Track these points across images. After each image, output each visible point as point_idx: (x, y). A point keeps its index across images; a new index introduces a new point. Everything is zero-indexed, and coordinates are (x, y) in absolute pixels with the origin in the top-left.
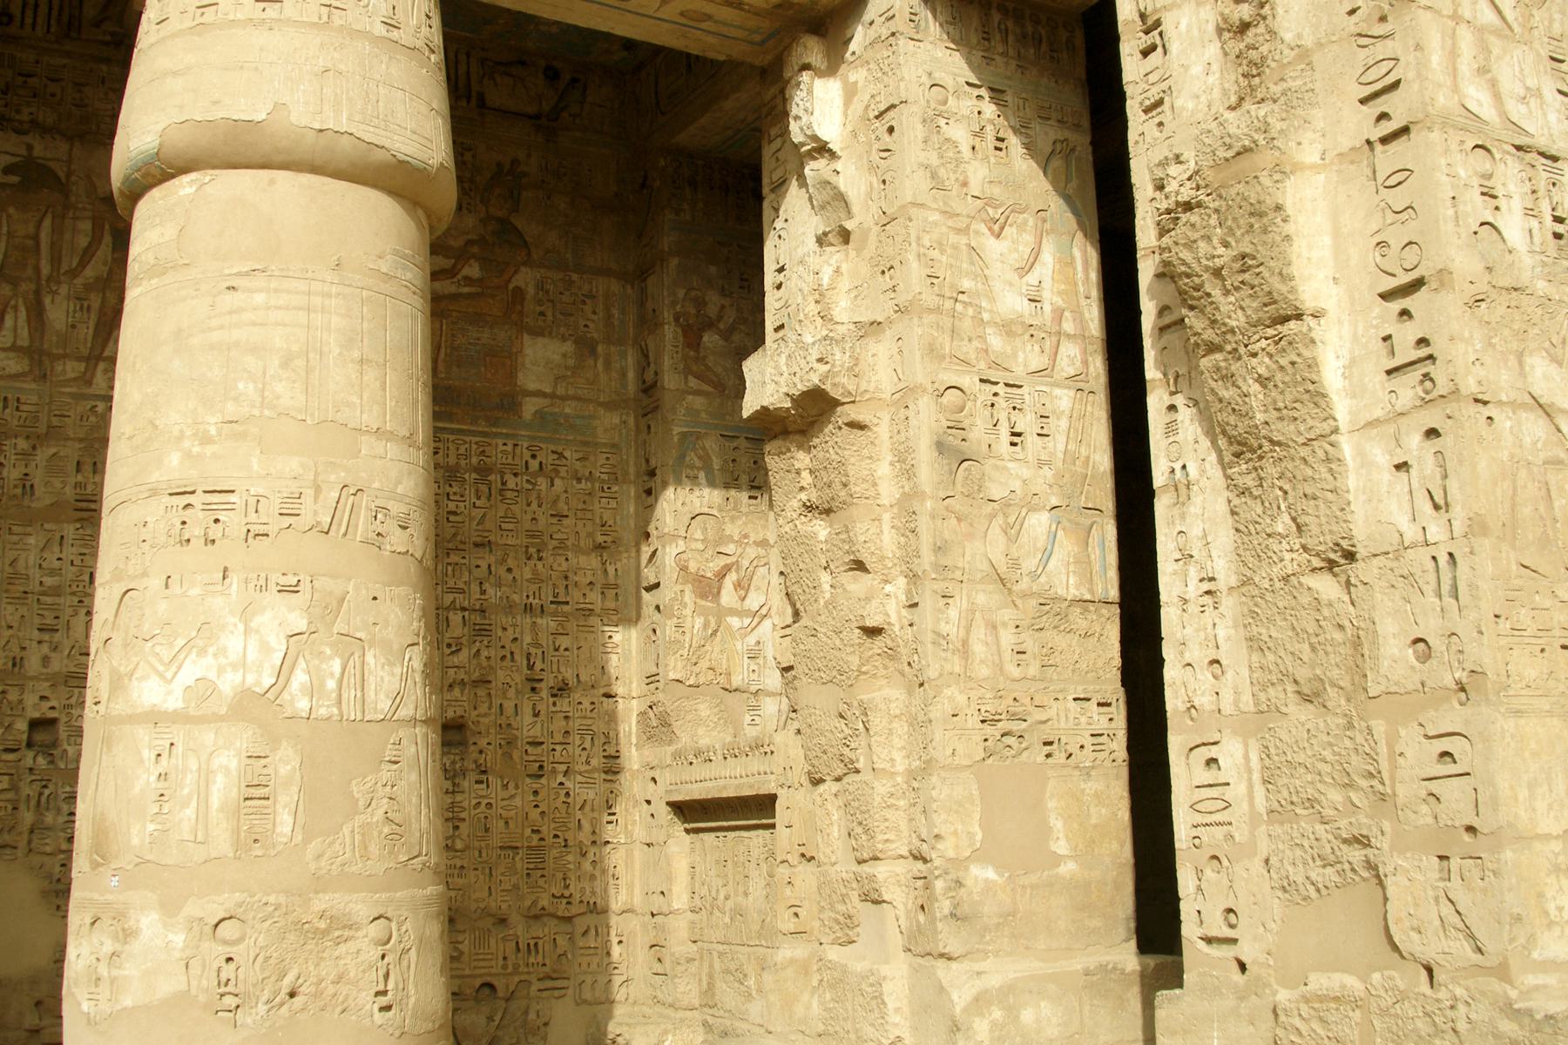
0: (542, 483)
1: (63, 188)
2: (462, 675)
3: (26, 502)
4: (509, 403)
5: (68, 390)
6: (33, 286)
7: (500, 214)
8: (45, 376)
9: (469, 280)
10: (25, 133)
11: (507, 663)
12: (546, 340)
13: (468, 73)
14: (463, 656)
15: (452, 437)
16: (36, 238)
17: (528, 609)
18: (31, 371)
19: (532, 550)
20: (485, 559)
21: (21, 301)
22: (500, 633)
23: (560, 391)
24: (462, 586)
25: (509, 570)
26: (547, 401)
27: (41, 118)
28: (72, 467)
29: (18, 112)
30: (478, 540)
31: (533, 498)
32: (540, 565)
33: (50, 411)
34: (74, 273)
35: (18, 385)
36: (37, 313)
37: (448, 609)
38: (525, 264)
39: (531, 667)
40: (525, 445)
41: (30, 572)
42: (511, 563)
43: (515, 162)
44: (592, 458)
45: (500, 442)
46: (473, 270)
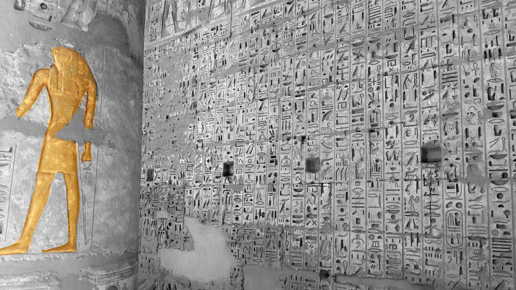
2: (434, 112)
11: (471, 98)
14: (436, 98)
17: (488, 55)
20: (449, 29)
22: (463, 77)
24: (432, 50)
28: (238, 47)
30: (444, 16)
32: (496, 20)
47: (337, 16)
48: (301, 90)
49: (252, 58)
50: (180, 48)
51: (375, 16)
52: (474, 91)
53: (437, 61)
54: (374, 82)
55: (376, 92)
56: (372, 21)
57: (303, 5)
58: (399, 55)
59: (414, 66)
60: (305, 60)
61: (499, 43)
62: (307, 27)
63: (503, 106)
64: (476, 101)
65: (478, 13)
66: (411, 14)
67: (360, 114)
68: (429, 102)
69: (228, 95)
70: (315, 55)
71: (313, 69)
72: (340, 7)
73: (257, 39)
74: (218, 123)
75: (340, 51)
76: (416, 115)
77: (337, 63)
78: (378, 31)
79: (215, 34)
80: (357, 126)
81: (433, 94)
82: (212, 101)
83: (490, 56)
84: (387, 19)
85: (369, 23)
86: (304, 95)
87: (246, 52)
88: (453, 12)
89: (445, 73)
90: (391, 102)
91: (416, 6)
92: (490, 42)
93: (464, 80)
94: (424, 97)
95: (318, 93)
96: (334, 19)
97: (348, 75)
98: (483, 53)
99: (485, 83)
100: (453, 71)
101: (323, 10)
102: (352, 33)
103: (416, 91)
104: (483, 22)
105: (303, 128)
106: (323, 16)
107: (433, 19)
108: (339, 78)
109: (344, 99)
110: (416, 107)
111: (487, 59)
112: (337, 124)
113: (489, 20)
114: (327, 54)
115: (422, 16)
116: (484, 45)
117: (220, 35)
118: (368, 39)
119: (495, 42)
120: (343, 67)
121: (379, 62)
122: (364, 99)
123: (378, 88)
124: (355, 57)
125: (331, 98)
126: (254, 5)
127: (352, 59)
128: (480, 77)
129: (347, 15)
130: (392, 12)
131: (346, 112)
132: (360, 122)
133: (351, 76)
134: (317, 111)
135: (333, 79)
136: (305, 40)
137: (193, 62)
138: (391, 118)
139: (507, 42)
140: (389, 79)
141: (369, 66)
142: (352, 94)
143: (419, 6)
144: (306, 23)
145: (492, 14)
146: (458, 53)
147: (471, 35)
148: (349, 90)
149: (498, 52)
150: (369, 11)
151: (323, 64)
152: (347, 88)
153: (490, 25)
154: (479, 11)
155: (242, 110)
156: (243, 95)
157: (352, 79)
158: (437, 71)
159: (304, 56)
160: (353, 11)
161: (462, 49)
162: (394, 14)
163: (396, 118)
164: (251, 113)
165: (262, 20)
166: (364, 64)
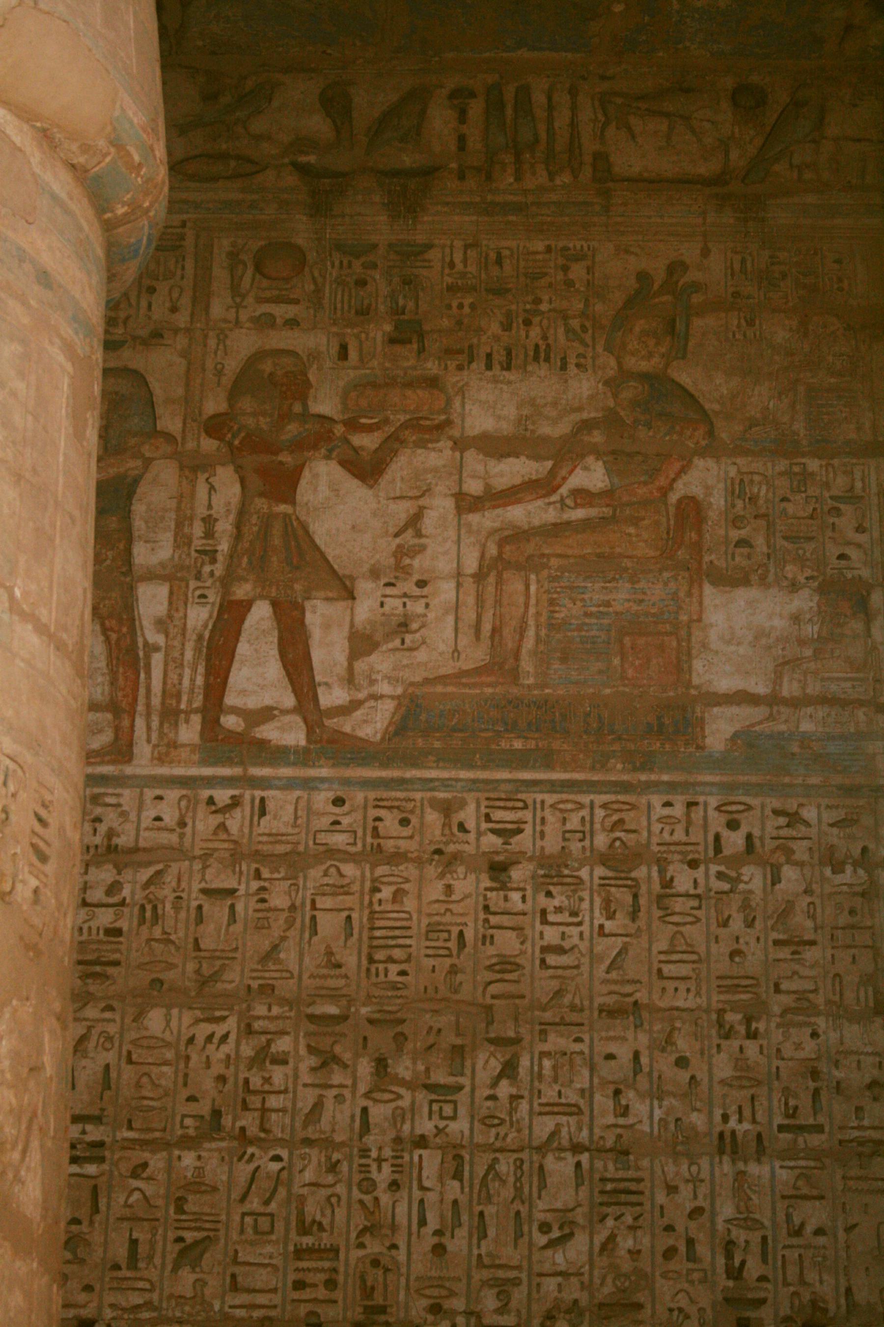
0: (753, 878)
2: (573, 1292)
4: (675, 721)
7: (644, 366)
9: (582, 496)
11: (679, 1264)
12: (754, 593)
13: (573, 125)
14: (578, 1249)
15: (550, 799)
17: (727, 1144)
19: (733, 1017)
20: (626, 1043)
22: (661, 1198)
23: (789, 688)
24: (572, 1097)
25: (682, 1062)
26: (760, 712)
30: (610, 1000)
31: (733, 909)
37: (542, 1149)
38: (703, 453)
39: (735, 1273)
40: (713, 802)
42: (683, 1044)
43: (676, 268)
44: (867, 820)
45: (656, 800)
46: (593, 476)
47: (253, 904)
48: (88, 1138)
51: (393, 942)
52: (690, 1242)
53: (585, 1133)
54: (380, 1160)
55: (385, 1199)
56: (380, 955)
57: (115, 825)
58: (467, 1089)
59: (513, 1135)
60: (112, 1029)
61: (759, 1117)
62: (126, 910)
63: (763, 1301)
64: (696, 1276)
65: (705, 1016)
66: (506, 965)
67: (327, 1264)
68: (559, 1258)
70: (155, 1020)
71: (146, 1069)
72: (266, 874)
75: (257, 1025)
76: (518, 1295)
77: (242, 1067)
78: (399, 993)
80: (310, 1307)
81: (572, 1234)
83: (734, 1152)
84: (431, 962)
85: (371, 960)
86: (102, 1160)
88: (638, 995)
89: (609, 1176)
90: (435, 1240)
91: (528, 945)
92: (734, 1108)
93: (662, 1207)
94: (543, 1240)
95: (161, 1165)
96: (240, 908)
97: (287, 1121)
98: (716, 1136)
99: (720, 1226)
100: (631, 1174)
101: (197, 866)
102: (305, 977)
103: (518, 1213)
104: (719, 1046)
105: (88, 1288)
106: (196, 886)
107: (577, 1001)
108: (249, 1121)
109: (267, 1203)
110: (519, 1268)
111: (726, 1158)
112: (235, 1287)
113: (736, 1043)
114: (206, 1029)
115: (544, 985)
116: (718, 1113)
118: (364, 1010)
119: (747, 1113)
120: (267, 1087)
121: (399, 1097)
122: (340, 1214)
123: (394, 1185)
124: (313, 1061)
125: (215, 1189)
127: (304, 1067)
128: (706, 1205)
129: (293, 908)
130: (449, 944)
131: (269, 1249)
132: (322, 1293)
133: (298, 1124)
134: (154, 1231)
135: (227, 1121)
136: (117, 956)
138: (435, 1292)
139: (778, 1120)
140: (431, 1162)
141: (365, 1103)
142: (296, 1189)
143: (537, 951)
144: (126, 892)
145: (742, 1029)
146: (646, 1120)
147: (684, 1076)
148: (285, 1174)
149: (754, 1144)
150: (371, 919)
151: (188, 1058)
152: (275, 1166)
153: (737, 1059)
154: (708, 1011)
157: (301, 1134)
158: (585, 1165)
159: (108, 1015)
160: (313, 902)
161: (658, 1114)
162: (455, 952)
163: (452, 1294)
166: (347, 1093)
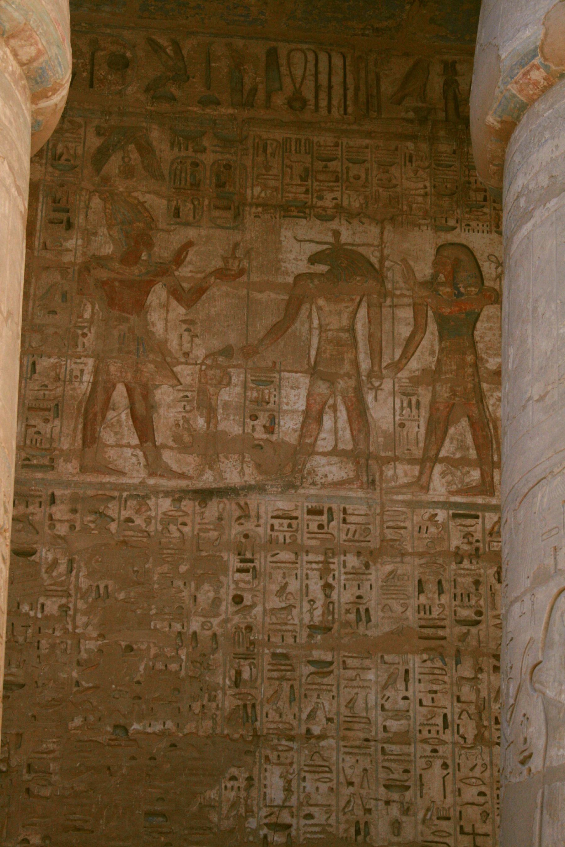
1: (377, 274)
3: (362, 629)
5: (400, 497)
6: (352, 383)
8: (373, 482)
10: (332, 218)
16: (352, 330)
18: (357, 477)
21: (339, 399)
27: (345, 203)
28: (412, 587)
29: (321, 198)
33: (382, 522)
34: (397, 366)
35: (342, 493)
36: (359, 414)
41: (372, 715)
49: (464, 629)
50: (172, 528)
69: (383, 708)
73: (477, 583)
74: (351, 784)
79: (321, 526)
82: (320, 714)
87: (442, 606)
117: (344, 537)
126: (458, 492)
137: (236, 583)
155: (438, 763)
156: (439, 721)
164: (471, 774)
165: (488, 539)
